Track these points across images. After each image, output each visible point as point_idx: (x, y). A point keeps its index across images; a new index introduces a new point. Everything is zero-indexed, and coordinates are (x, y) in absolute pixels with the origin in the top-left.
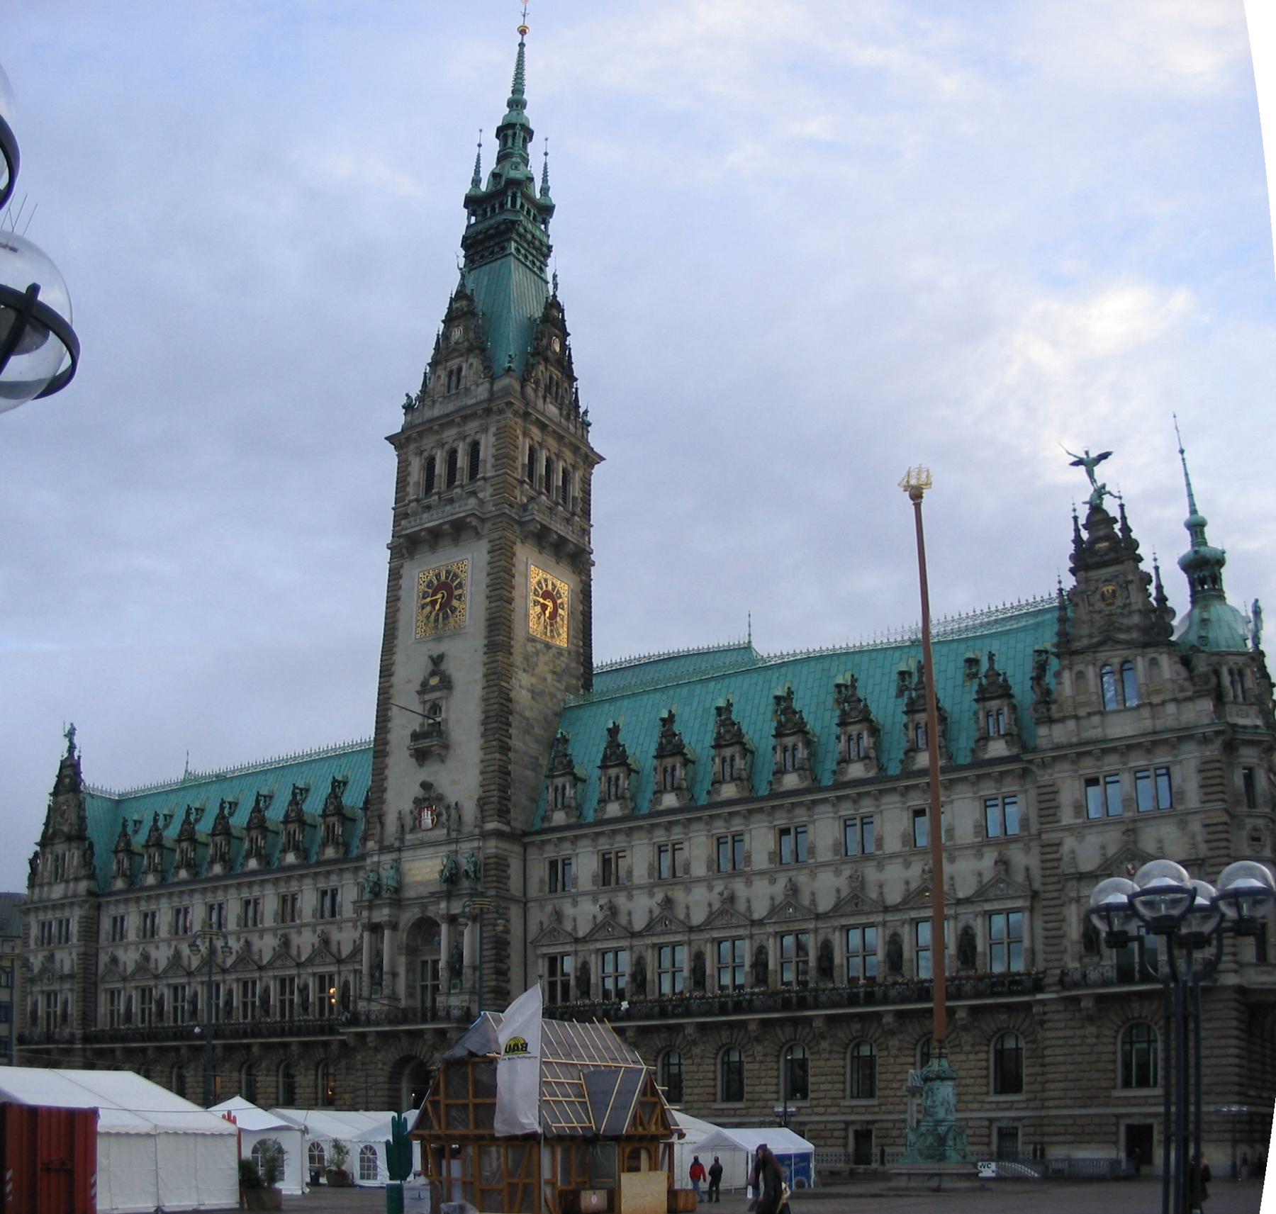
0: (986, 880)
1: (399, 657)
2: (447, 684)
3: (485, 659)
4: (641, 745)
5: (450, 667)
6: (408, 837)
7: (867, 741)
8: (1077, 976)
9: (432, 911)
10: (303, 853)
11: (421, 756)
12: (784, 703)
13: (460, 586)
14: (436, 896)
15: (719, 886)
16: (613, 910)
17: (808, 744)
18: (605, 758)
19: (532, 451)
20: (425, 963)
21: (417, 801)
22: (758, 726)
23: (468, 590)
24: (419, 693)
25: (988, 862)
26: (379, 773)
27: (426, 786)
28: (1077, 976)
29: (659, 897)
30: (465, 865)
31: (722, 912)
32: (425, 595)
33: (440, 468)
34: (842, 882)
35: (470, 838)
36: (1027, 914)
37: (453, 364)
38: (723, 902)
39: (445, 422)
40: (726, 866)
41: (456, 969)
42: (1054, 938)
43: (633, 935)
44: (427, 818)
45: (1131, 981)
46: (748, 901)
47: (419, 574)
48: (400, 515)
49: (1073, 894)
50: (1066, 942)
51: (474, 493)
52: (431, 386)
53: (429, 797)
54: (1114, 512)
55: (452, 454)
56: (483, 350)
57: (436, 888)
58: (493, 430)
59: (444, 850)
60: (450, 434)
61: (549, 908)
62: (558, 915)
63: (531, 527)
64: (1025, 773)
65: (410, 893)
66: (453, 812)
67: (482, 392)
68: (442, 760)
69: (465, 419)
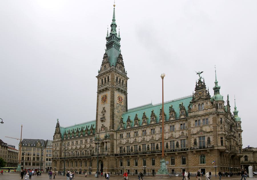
0: (180, 135)
2: (105, 111)
3: (110, 107)
4: (132, 119)
6: (100, 132)
8: (193, 148)
11: (102, 121)
13: (107, 97)
14: (104, 139)
16: (128, 141)
17: (155, 117)
18: (127, 120)
19: (117, 77)
20: (103, 148)
21: (101, 127)
23: (108, 98)
24: (102, 113)
25: (180, 133)
26: (97, 124)
27: (103, 125)
28: (193, 148)
29: (134, 139)
30: (108, 135)
31: (143, 140)
32: (102, 99)
33: (104, 81)
35: (109, 132)
36: (186, 140)
38: (143, 139)
40: (128, 137)
42: (190, 143)
43: (131, 144)
45: (201, 149)
46: (147, 139)
47: (101, 96)
49: (193, 137)
50: (191, 144)
51: (108, 84)
53: (103, 127)
57: (104, 138)
58: (111, 75)
59: (105, 133)
61: (120, 141)
62: (121, 141)
63: (117, 89)
66: (106, 128)
68: (104, 121)
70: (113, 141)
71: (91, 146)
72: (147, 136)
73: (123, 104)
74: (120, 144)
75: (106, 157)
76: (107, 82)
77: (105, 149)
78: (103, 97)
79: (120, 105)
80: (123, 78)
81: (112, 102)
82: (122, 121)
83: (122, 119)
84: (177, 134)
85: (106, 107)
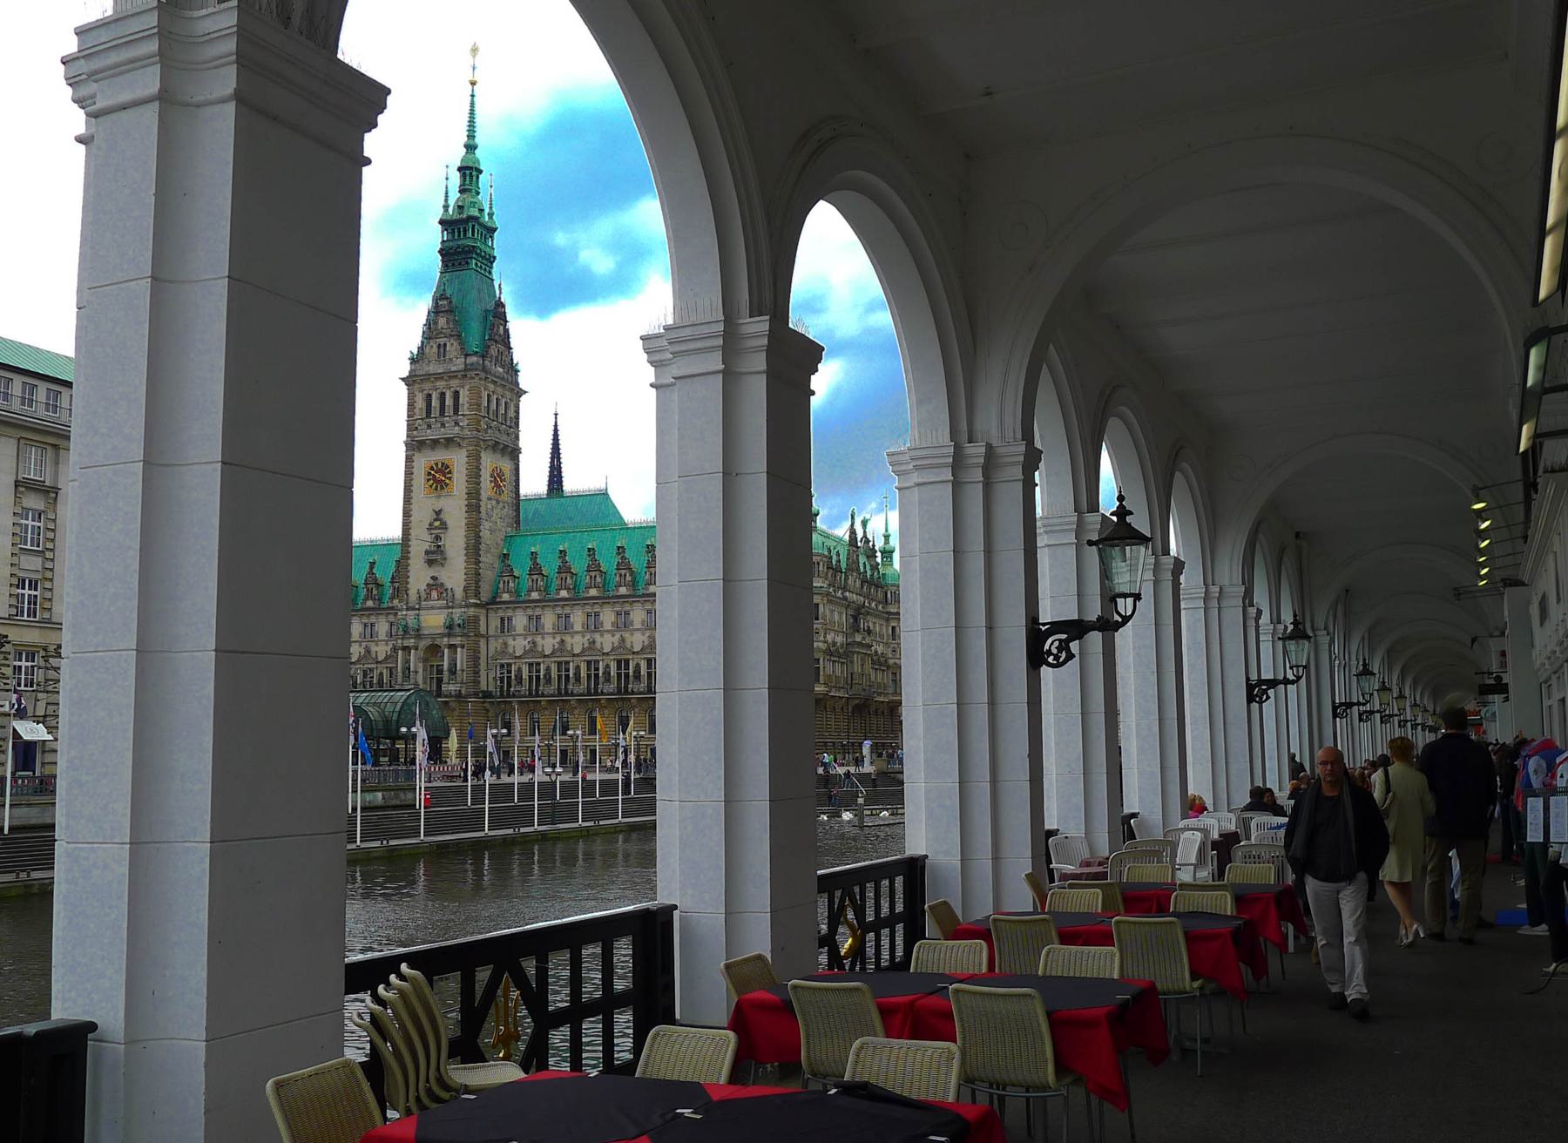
2: (444, 526)
4: (550, 566)
9: (438, 642)
11: (430, 563)
14: (442, 635)
22: (608, 562)
23: (455, 476)
29: (558, 639)
30: (457, 621)
33: (435, 403)
34: (645, 638)
37: (442, 341)
39: (439, 377)
41: (453, 671)
44: (434, 594)
51: (457, 424)
55: (443, 395)
56: (459, 336)
60: (440, 384)
67: (458, 364)
70: (477, 643)
71: (368, 651)
72: (602, 634)
73: (507, 496)
74: (504, 653)
75: (453, 705)
76: (449, 411)
77: (446, 673)
80: (508, 394)
81: (474, 496)
82: (507, 570)
85: (446, 509)
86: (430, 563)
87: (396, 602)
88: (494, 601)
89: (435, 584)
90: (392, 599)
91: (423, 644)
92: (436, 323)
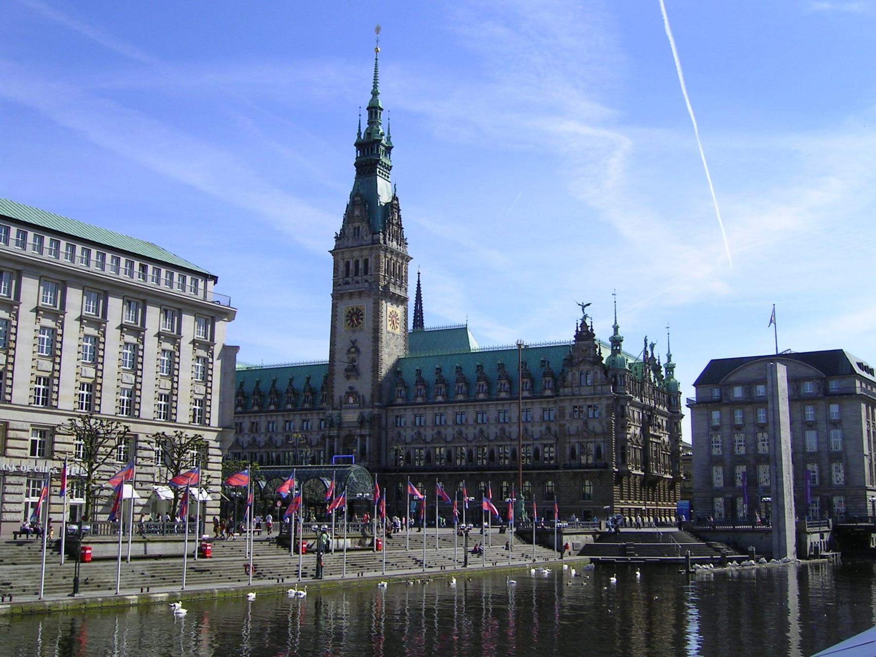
1: (338, 339)
2: (358, 351)
5: (358, 345)
7: (507, 386)
9: (352, 433)
10: (295, 404)
11: (348, 377)
12: (480, 368)
13: (362, 315)
15: (457, 428)
16: (419, 433)
23: (365, 316)
25: (543, 428)
29: (436, 431)
32: (347, 316)
33: (352, 267)
35: (369, 407)
43: (427, 443)
44: (351, 400)
48: (335, 284)
51: (366, 281)
52: (346, 232)
54: (589, 324)
55: (357, 263)
58: (373, 256)
60: (356, 254)
62: (399, 434)
64: (556, 402)
65: (345, 425)
67: (368, 238)
69: (362, 250)
76: (361, 272)
78: (349, 312)
79: (394, 334)
83: (399, 373)
84: (537, 430)
86: (348, 377)
87: (324, 405)
88: (391, 404)
89: (351, 392)
90: (322, 401)
91: (344, 433)
92: (353, 213)
